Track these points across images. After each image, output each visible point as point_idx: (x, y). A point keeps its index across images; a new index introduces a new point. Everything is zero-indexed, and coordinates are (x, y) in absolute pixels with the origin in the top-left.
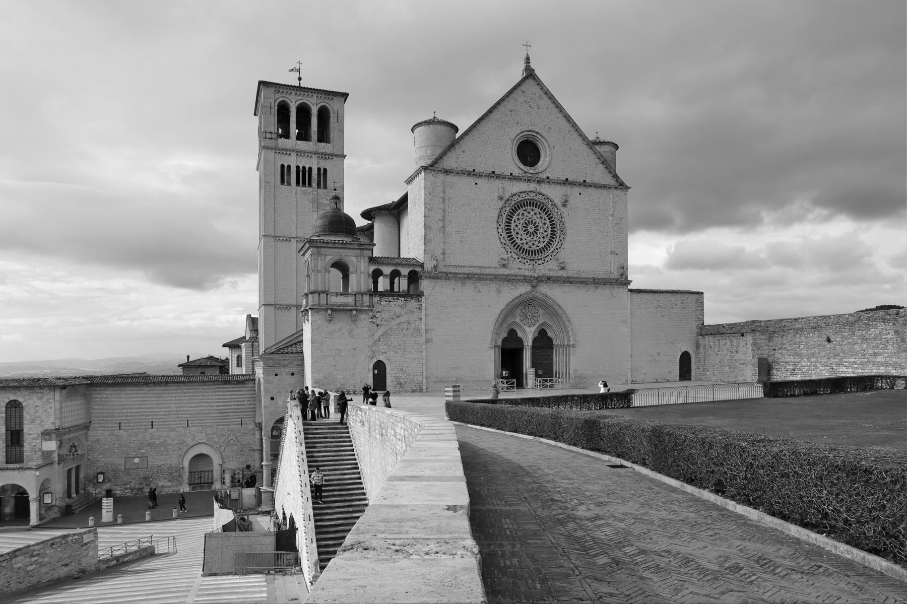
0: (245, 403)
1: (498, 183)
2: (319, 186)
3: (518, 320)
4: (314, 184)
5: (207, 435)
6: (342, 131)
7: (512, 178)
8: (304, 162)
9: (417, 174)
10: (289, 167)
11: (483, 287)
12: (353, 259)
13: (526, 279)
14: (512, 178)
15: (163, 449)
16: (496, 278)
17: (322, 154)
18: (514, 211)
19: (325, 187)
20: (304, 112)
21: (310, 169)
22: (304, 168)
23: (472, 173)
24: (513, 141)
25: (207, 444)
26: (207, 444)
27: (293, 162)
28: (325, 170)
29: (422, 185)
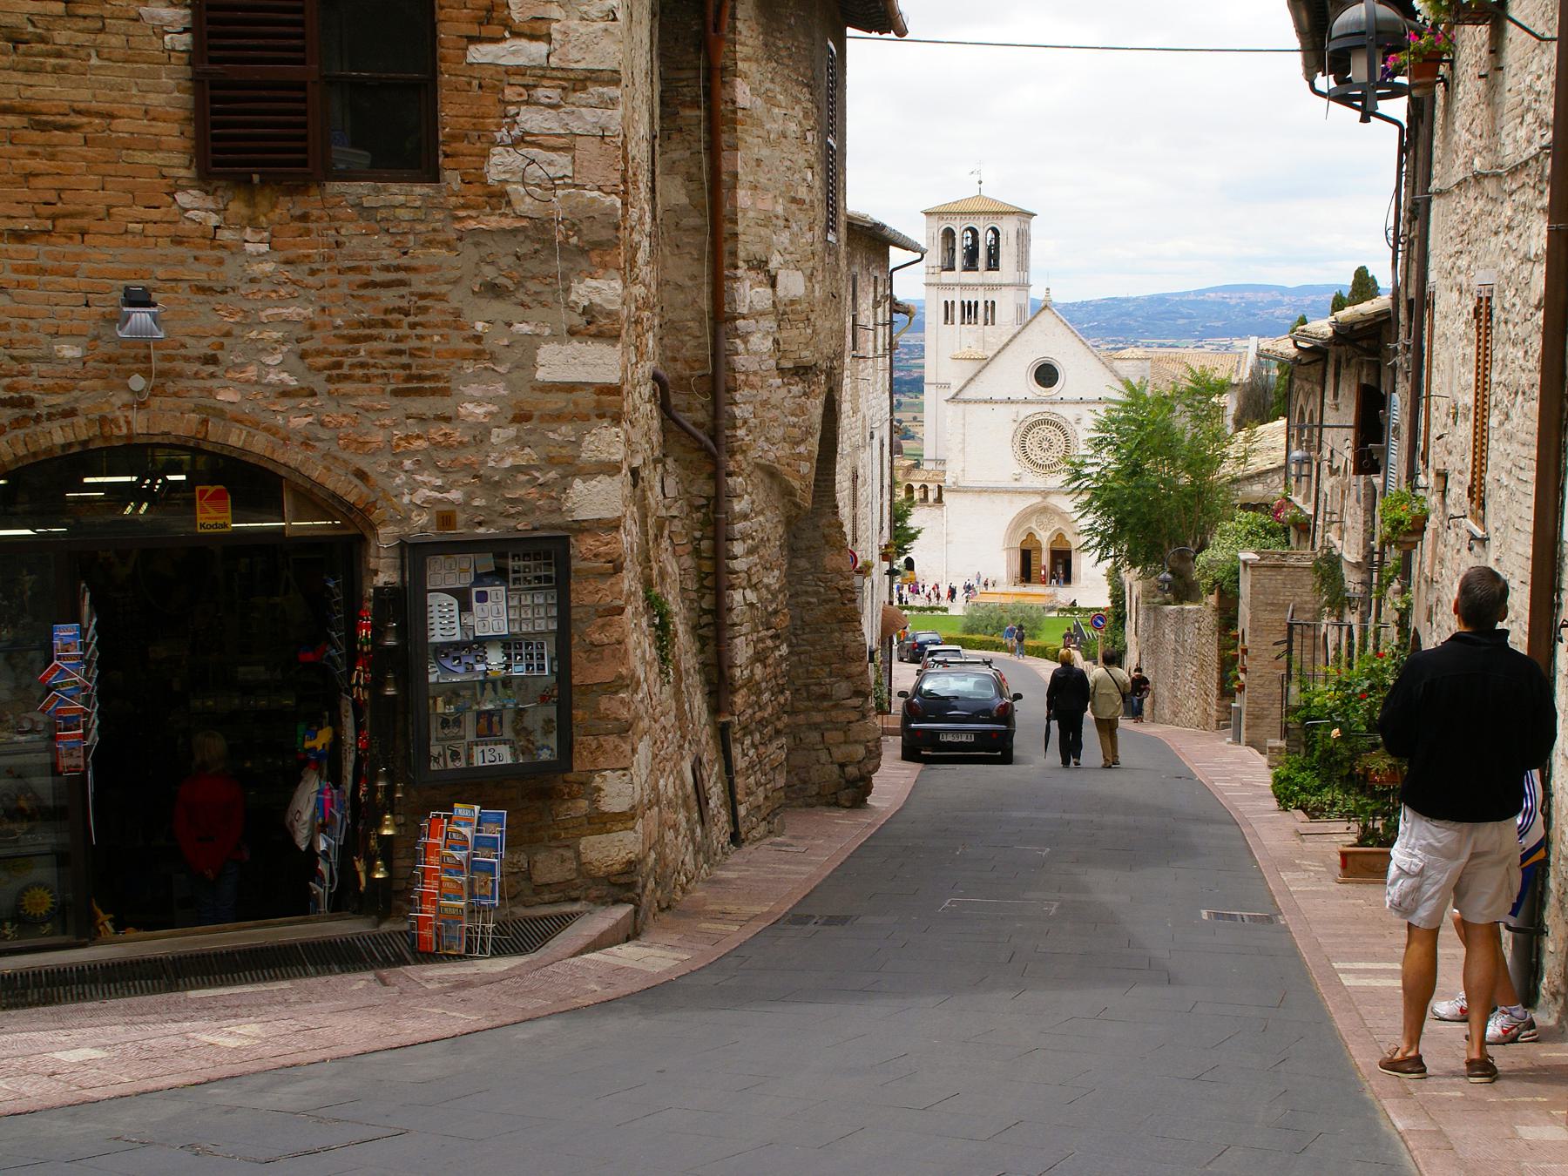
1: (1013, 406)
2: (986, 324)
3: (1034, 526)
4: (981, 320)
7: (1026, 401)
8: (969, 296)
10: (953, 302)
11: (997, 498)
13: (1036, 492)
14: (1026, 401)
16: (1007, 491)
18: (1029, 429)
19: (993, 324)
21: (976, 303)
22: (969, 302)
23: (991, 401)
27: (957, 297)
28: (993, 303)
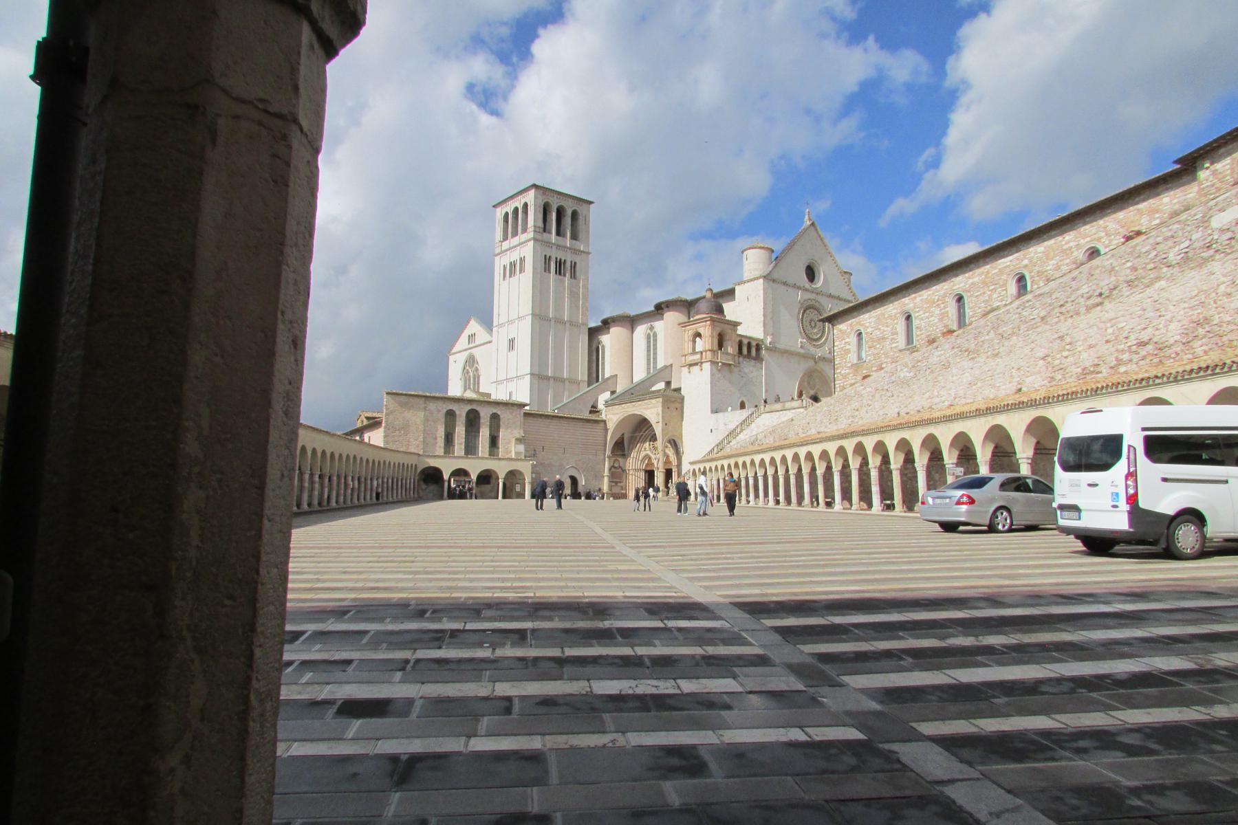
0: (599, 439)
5: (576, 461)
6: (588, 232)
8: (561, 255)
9: (760, 278)
10: (550, 257)
12: (730, 331)
15: (549, 469)
16: (798, 354)
17: (574, 250)
19: (575, 278)
20: (560, 212)
23: (785, 284)
24: (804, 264)
25: (576, 468)
26: (576, 468)
27: (555, 254)
28: (575, 263)
29: (762, 287)
